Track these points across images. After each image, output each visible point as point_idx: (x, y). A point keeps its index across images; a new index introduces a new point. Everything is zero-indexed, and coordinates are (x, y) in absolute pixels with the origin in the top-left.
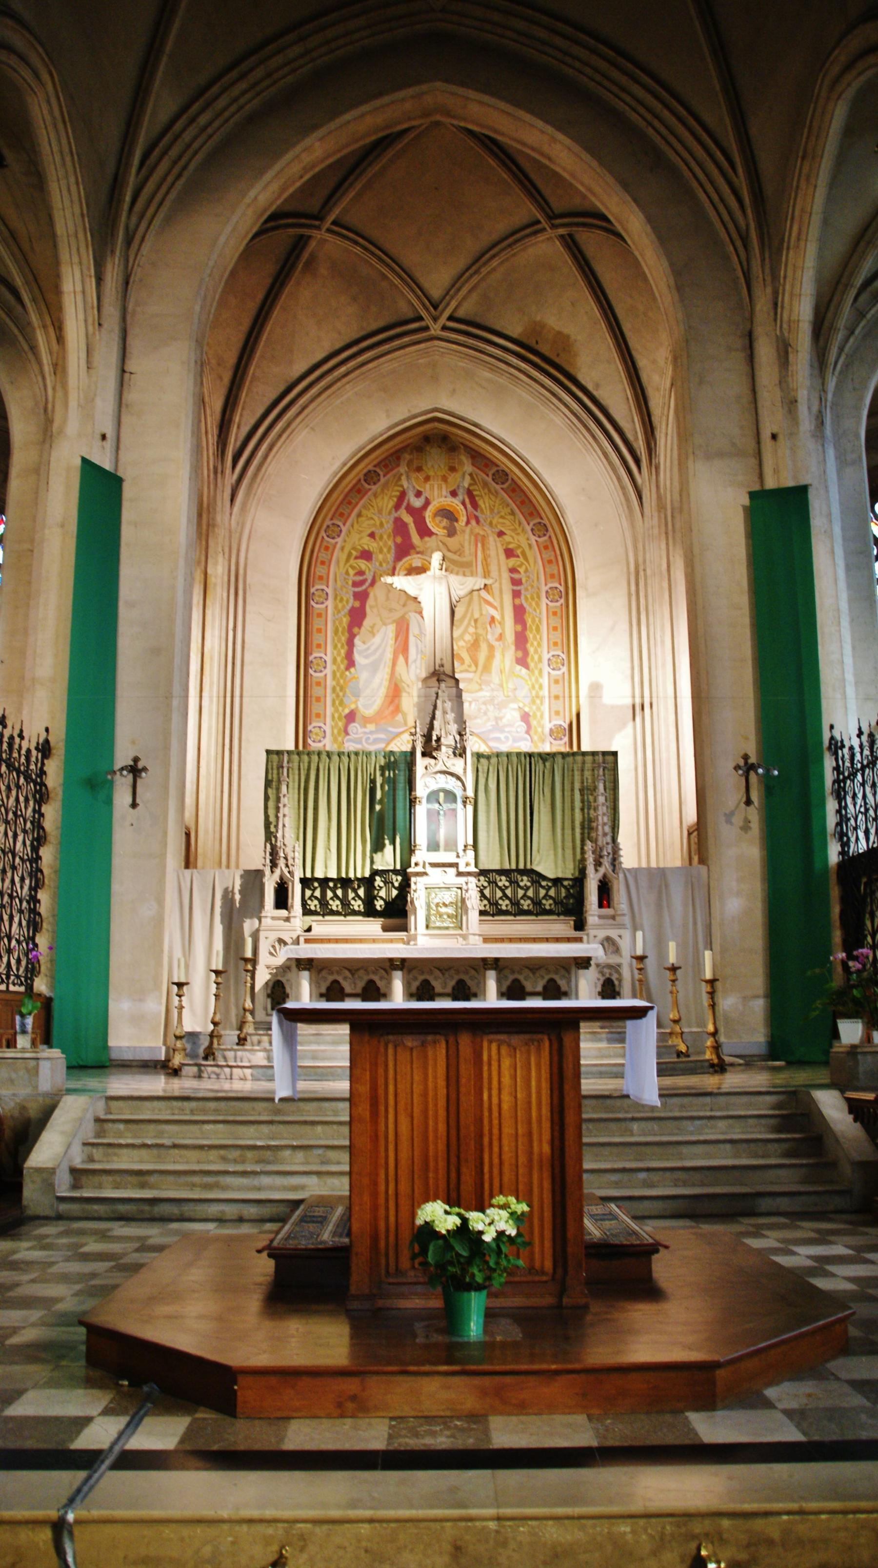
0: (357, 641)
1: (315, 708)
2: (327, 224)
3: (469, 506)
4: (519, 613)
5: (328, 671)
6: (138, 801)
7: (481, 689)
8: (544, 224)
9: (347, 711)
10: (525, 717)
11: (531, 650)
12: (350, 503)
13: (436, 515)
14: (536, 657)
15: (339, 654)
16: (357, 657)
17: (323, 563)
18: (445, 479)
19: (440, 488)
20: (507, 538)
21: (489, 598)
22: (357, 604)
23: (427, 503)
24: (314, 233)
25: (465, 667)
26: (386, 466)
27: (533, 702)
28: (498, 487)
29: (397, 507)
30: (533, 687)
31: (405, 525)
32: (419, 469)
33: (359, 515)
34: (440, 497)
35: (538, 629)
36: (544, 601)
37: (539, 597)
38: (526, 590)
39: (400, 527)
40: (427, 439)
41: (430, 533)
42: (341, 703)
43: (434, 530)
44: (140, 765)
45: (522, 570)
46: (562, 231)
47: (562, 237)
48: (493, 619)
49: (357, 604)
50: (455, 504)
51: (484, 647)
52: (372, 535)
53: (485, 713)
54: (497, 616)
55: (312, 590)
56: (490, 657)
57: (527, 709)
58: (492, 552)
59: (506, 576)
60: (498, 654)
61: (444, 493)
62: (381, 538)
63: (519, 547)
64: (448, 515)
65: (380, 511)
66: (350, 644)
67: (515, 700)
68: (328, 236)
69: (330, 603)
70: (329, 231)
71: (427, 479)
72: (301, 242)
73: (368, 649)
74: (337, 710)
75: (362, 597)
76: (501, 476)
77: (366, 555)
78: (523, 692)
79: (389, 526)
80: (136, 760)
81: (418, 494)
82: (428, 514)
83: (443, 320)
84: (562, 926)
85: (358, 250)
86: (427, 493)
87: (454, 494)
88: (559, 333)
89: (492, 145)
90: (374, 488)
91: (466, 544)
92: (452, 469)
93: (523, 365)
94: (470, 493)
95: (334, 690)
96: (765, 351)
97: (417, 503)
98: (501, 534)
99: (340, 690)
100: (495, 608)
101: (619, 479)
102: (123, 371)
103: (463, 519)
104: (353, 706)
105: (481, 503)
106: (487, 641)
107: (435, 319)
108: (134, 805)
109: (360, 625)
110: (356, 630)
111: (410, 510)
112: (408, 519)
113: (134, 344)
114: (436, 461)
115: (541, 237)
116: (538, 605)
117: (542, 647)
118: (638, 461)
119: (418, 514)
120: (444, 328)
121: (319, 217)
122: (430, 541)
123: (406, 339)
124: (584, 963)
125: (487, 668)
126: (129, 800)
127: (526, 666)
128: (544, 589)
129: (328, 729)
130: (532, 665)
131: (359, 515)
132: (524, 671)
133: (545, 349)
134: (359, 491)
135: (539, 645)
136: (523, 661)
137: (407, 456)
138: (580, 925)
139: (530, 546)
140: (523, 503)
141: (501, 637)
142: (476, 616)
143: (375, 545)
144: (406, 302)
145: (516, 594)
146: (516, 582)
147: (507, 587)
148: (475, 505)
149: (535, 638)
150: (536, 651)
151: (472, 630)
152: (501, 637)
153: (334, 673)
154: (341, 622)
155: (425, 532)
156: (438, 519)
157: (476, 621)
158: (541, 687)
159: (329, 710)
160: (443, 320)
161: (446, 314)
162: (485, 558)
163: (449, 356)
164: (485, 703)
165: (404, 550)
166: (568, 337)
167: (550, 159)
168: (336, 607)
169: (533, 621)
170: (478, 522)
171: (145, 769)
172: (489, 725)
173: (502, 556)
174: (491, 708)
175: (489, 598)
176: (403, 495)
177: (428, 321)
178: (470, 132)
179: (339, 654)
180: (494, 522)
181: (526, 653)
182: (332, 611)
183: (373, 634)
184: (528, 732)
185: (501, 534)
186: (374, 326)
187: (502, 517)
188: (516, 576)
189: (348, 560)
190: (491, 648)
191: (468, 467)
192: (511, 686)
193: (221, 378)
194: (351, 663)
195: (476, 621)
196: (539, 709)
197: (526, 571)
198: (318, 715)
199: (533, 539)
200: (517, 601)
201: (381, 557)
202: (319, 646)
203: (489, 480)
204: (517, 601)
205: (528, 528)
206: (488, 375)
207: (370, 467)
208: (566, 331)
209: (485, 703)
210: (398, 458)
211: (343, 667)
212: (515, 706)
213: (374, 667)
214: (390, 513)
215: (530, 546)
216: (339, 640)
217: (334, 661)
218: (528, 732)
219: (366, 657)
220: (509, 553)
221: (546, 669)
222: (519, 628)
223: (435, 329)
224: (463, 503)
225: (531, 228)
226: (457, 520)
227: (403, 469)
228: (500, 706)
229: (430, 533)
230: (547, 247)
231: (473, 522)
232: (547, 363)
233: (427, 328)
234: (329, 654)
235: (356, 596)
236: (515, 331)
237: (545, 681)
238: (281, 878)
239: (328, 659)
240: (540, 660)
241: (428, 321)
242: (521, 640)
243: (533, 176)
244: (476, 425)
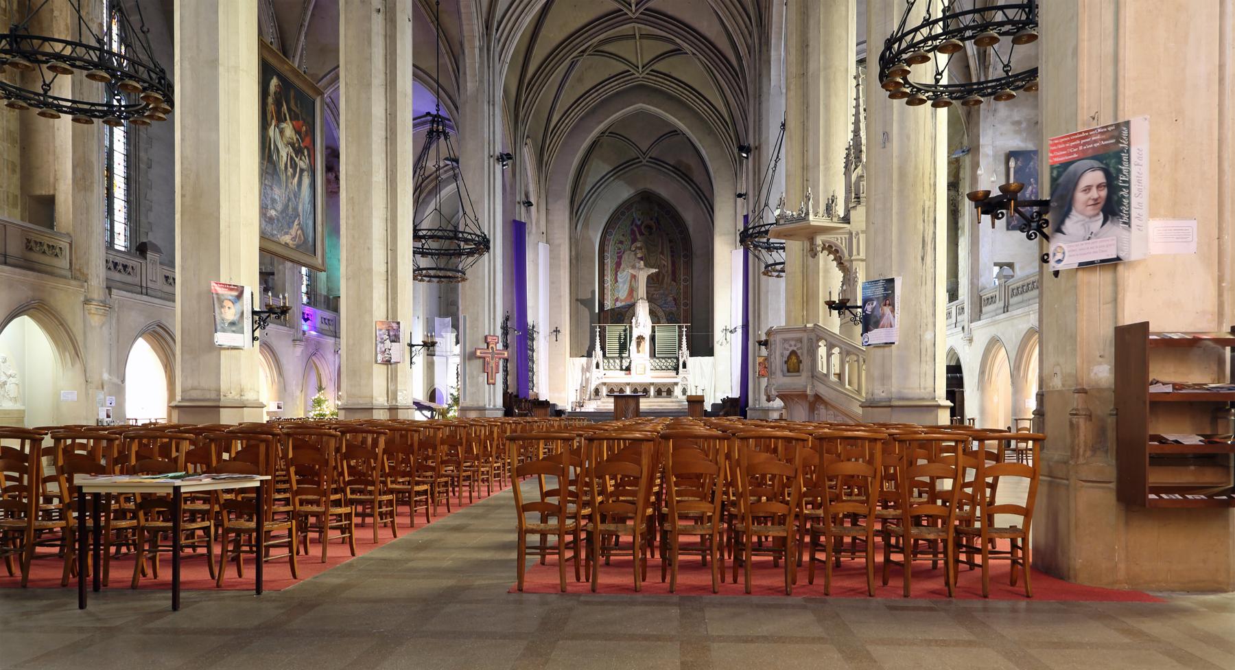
4: (673, 264)
10: (675, 299)
39: (633, 232)
50: (652, 223)
75: (620, 258)
77: (621, 242)
84: (674, 374)
113: (550, 200)
124: (676, 384)
136: (674, 280)
144: (633, 153)
165: (634, 241)
194: (616, 281)
213: (624, 283)
220: (670, 241)
223: (644, 162)
234: (608, 278)
242: (674, 272)
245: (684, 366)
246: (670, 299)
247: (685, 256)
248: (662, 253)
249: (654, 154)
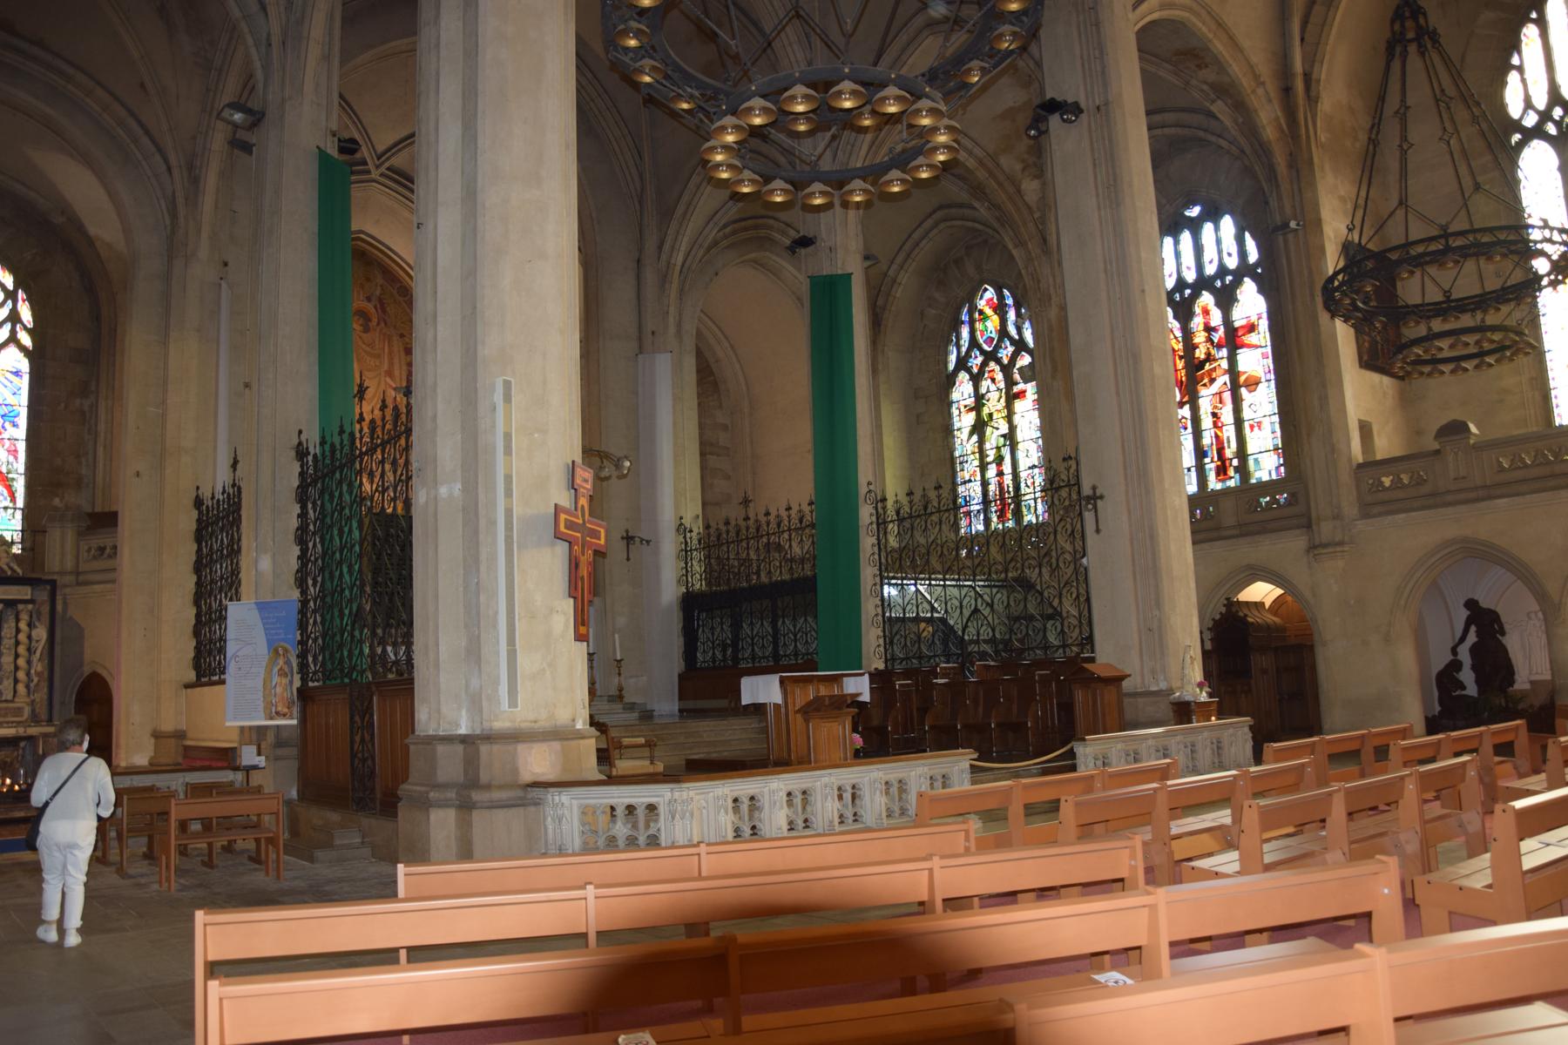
18: (362, 286)
50: (370, 307)
87: (369, 299)
92: (368, 280)
94: (380, 300)
96: (650, 277)
120: (382, 175)
148: (384, 311)
160: (383, 169)
161: (387, 165)
162: (390, 353)
177: (371, 166)
191: (380, 280)
223: (375, 174)
248: (390, 373)
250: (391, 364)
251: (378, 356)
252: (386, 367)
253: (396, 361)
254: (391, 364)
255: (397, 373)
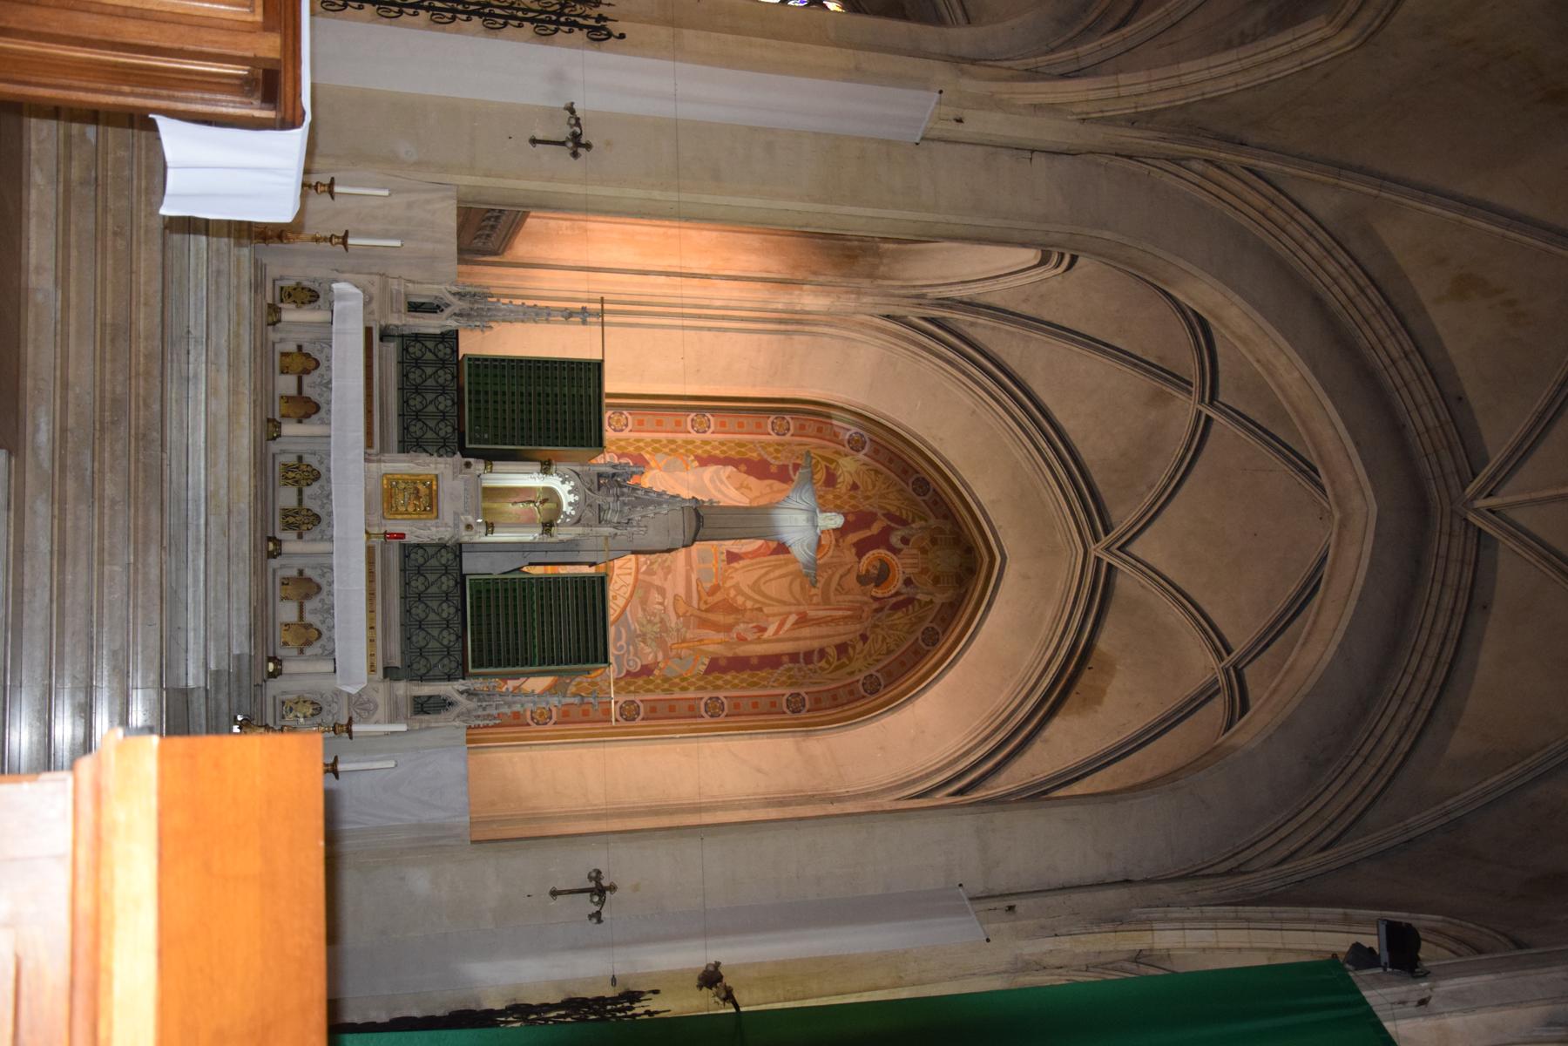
0: (730, 469)
1: (650, 419)
2: (1206, 411)
3: (894, 600)
4: (771, 661)
5: (694, 435)
6: (539, 146)
7: (678, 616)
8: (1229, 660)
9: (647, 457)
10: (646, 671)
11: (728, 677)
12: (891, 461)
13: (881, 560)
14: (720, 683)
15: (714, 448)
16: (711, 470)
17: (820, 430)
18: (924, 571)
19: (914, 566)
20: (859, 646)
21: (788, 625)
22: (773, 469)
23: (895, 551)
24: (1196, 396)
25: (705, 597)
26: (935, 503)
27: (666, 680)
28: (919, 634)
29: (889, 516)
30: (683, 680)
31: (868, 526)
32: (934, 541)
33: (877, 472)
34: (902, 567)
35: (754, 685)
36: (788, 691)
37: (791, 685)
38: (800, 670)
40: (970, 550)
41: (860, 555)
42: (656, 451)
43: (864, 560)
44: (581, 151)
45: (823, 664)
46: (1222, 679)
47: (1216, 681)
48: (764, 630)
49: (773, 469)
50: (897, 584)
51: (730, 619)
52: (855, 487)
53: (649, 621)
54: (766, 635)
55: (788, 417)
56: (717, 627)
57: (656, 672)
58: (841, 629)
59: (816, 644)
60: (722, 636)
61: (908, 571)
62: (852, 497)
63: (850, 660)
64: (882, 575)
65: (883, 496)
66: (726, 461)
67: (667, 658)
68: (1192, 414)
69: (774, 437)
70: (1200, 413)
71: (924, 551)
72: (1183, 383)
73: (722, 482)
74: (647, 444)
76: (932, 638)
78: (675, 668)
79: (865, 506)
80: (588, 146)
81: (905, 541)
82: (882, 552)
83: (1107, 558)
85: (1179, 451)
86: (906, 550)
87: (908, 582)
88: (1104, 692)
89: (1311, 588)
90: (910, 489)
91: (850, 597)
92: (936, 580)
93: (1063, 652)
94: (910, 601)
95: (673, 442)
96: (1110, 896)
97: (895, 540)
98: (864, 638)
99: (673, 449)
100: (777, 632)
101: (939, 770)
102: (1033, 151)
103: (879, 593)
104: (652, 464)
105: (900, 614)
106: (737, 623)
107: (1107, 549)
108: (534, 141)
109: (748, 472)
110: (743, 467)
111: (886, 531)
112: (875, 529)
114: (946, 561)
115: (1211, 659)
116: (782, 684)
117: (729, 690)
118: (960, 792)
119: (881, 540)
121: (1211, 403)
122: (849, 556)
123: (1082, 517)
125: (704, 623)
126: (539, 137)
127: (708, 671)
128: (802, 691)
129: (626, 434)
130: (710, 678)
131: (877, 472)
132: (703, 668)
133: (1085, 678)
134: (905, 472)
135: (735, 687)
136: (715, 666)
137: (948, 527)
138: (390, 673)
139: (852, 673)
140: (903, 664)
141: (742, 640)
142: (766, 610)
143: (844, 490)
144: (1123, 516)
145: (794, 657)
146: (808, 655)
147: (802, 646)
148: (896, 607)
149: (743, 681)
150: (727, 682)
151: (749, 604)
152: (742, 640)
153: (692, 442)
154: (751, 450)
155: (862, 548)
156: (878, 564)
157: (760, 610)
158: (684, 689)
159: (647, 436)
160: (1107, 558)
161: (1115, 562)
162: (833, 620)
163: (1067, 570)
164: (662, 621)
166: (1099, 701)
167: (1304, 644)
168: (769, 444)
169: (763, 679)
170: (876, 611)
171: (575, 155)
172: (635, 626)
173: (838, 640)
174: (656, 628)
175: (788, 625)
176: (904, 523)
177: (1105, 541)
178: (1324, 558)
179: (714, 448)
180: (878, 630)
181: (724, 670)
182: (764, 439)
183: (740, 487)
184: (628, 673)
185: (864, 638)
186: (1097, 479)
187: (884, 639)
188: (815, 657)
189: (823, 458)
190: (728, 628)
191: (940, 599)
192: (684, 653)
193: (1026, 300)
194: (705, 461)
195: (760, 610)
196: (657, 687)
197: (822, 669)
198: (641, 423)
199: (860, 677)
200: (785, 659)
201: (830, 497)
202: (723, 424)
203: (927, 624)
204: (785, 659)
205: (872, 671)
206: (1049, 613)
207: (933, 484)
208: (1106, 700)
209: (662, 621)
210: (945, 517)
211: (699, 452)
212: (660, 658)
214: (881, 508)
215: (852, 673)
216: (730, 449)
217: (706, 442)
218: (628, 673)
219: (712, 480)
220: (842, 649)
221: (706, 695)
222: (755, 661)
223: (1096, 550)
224: (897, 594)
225: (1222, 646)
226: (877, 586)
227: (933, 522)
228: (660, 642)
229: (860, 555)
230: (1202, 665)
231: (876, 605)
232: (1067, 681)
233: (1097, 539)
234: (714, 435)
235: (784, 468)
236: (1103, 644)
237: (691, 694)
238: (448, 305)
239: (708, 436)
240: (717, 688)
241: (1105, 541)
242: (739, 664)
243: (1281, 638)
244: (989, 605)
245: (423, 706)
246: (649, 654)
247: (796, 704)
248: (803, 620)
249: (1128, 581)
250: (819, 622)
251: (826, 600)
252: (812, 614)
253: (824, 630)
254: (819, 622)
255: (806, 632)
